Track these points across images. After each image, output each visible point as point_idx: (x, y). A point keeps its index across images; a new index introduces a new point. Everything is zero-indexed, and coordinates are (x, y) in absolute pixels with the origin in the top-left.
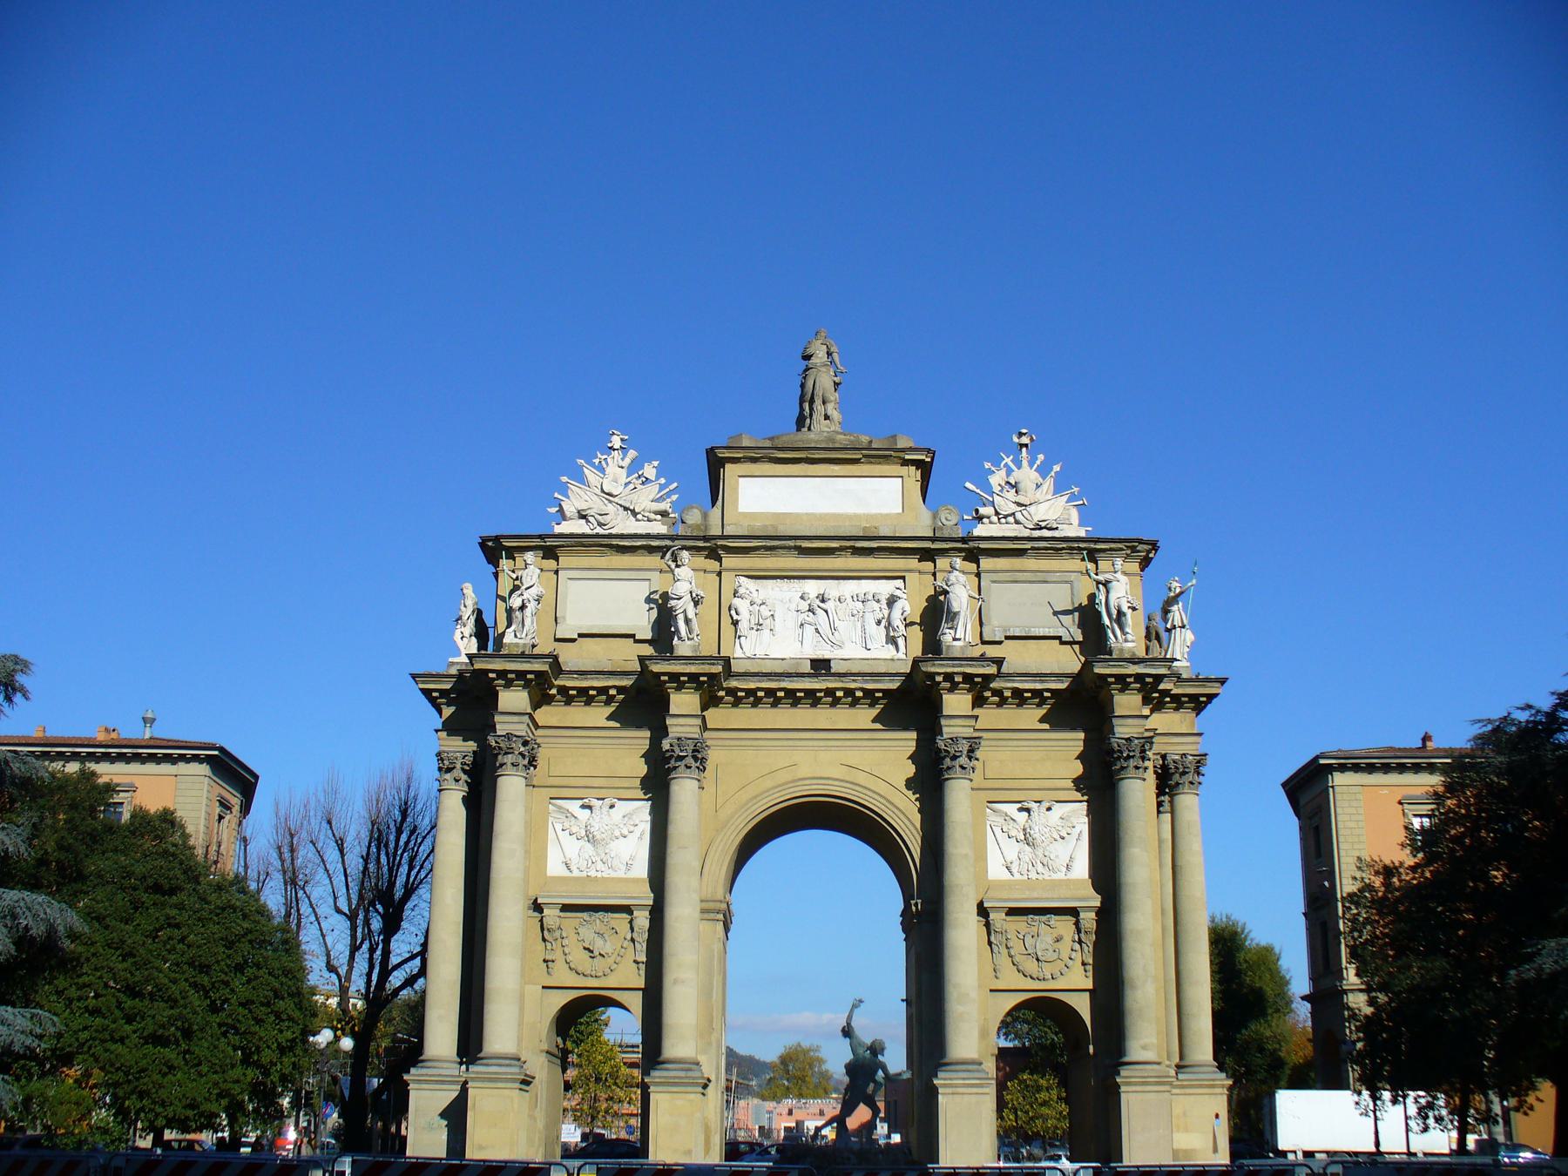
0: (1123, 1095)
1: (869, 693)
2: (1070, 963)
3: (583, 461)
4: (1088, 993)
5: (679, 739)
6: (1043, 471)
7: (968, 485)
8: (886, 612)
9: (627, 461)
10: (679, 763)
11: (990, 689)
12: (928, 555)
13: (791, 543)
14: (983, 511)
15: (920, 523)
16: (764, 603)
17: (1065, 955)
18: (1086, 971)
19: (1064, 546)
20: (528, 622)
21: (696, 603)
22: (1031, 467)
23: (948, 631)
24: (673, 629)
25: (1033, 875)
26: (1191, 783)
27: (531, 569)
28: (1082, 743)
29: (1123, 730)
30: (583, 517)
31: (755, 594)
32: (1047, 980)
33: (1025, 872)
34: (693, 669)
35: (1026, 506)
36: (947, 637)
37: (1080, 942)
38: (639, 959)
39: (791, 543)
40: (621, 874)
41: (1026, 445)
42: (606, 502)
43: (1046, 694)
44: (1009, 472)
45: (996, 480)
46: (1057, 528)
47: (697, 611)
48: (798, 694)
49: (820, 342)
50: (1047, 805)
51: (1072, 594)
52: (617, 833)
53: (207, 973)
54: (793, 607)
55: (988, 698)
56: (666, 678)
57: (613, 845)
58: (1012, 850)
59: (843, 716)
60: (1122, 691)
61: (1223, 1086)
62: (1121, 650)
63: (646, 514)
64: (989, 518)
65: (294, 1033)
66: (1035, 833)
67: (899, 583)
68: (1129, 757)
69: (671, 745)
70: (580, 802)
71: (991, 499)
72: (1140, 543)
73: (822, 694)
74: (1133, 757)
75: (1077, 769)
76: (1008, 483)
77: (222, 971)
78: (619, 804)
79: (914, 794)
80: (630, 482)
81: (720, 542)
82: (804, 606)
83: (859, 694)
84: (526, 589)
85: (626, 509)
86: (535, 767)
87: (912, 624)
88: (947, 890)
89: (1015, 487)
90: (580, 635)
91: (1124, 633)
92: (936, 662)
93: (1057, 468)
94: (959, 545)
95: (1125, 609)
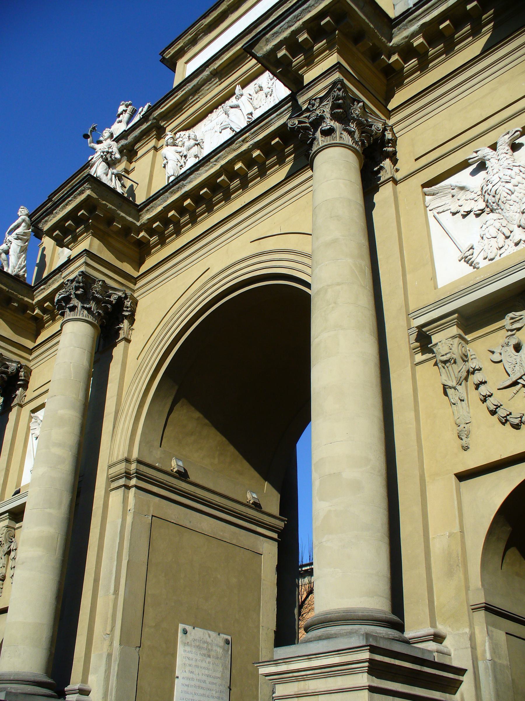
13: (206, 73)
39: (206, 73)
92: (267, 36)
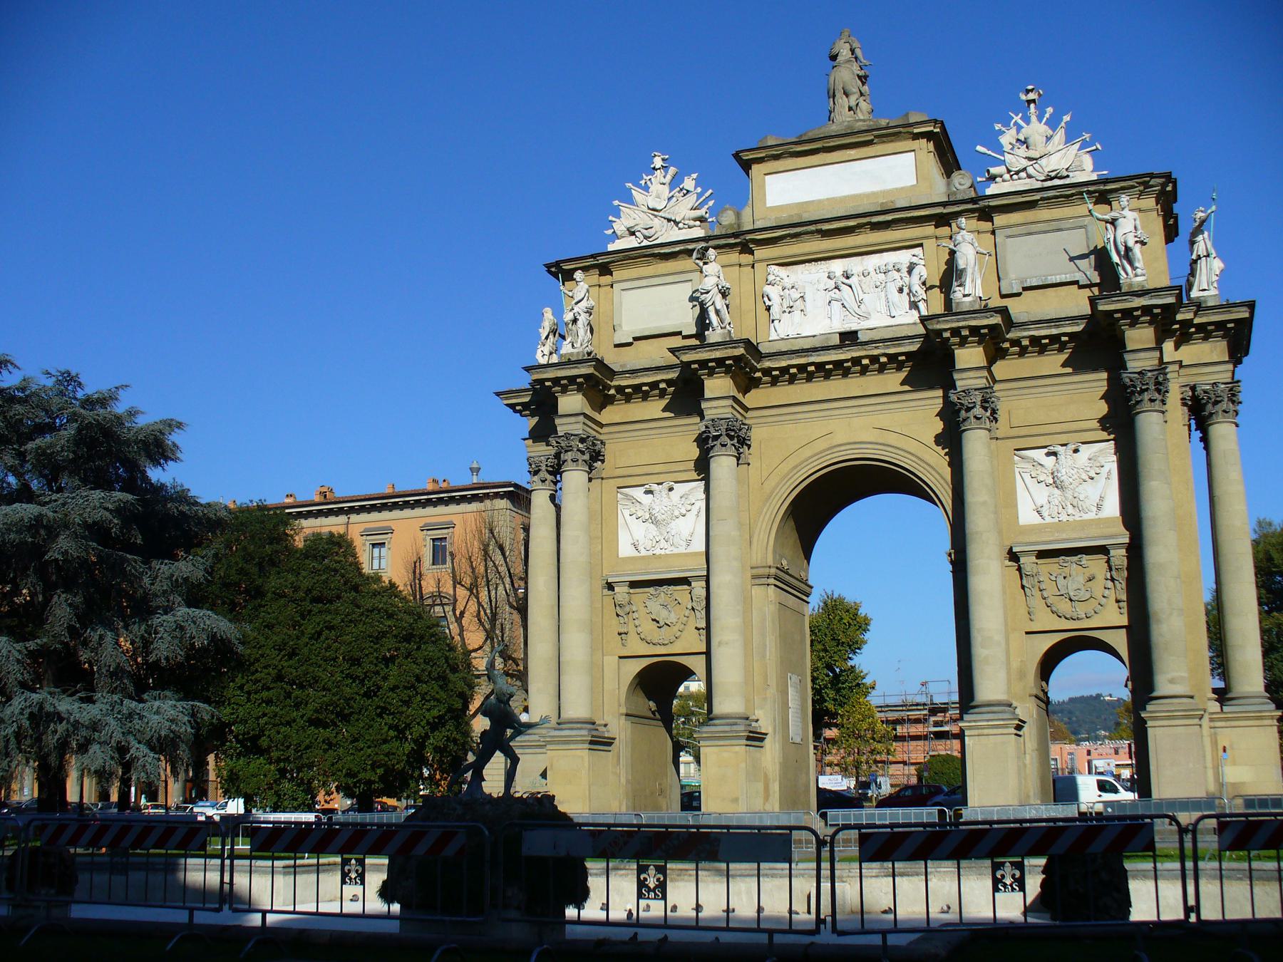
0: (1150, 731)
1: (892, 358)
2: (1103, 601)
3: (630, 185)
4: (1124, 630)
5: (713, 420)
6: (1053, 124)
7: (979, 148)
8: (907, 280)
9: (669, 177)
10: (715, 443)
11: (1007, 340)
12: (942, 220)
13: (812, 228)
14: (993, 170)
15: (936, 189)
16: (793, 287)
17: (1098, 594)
18: (1120, 608)
19: (1074, 191)
20: (581, 332)
21: (724, 294)
22: (1040, 122)
23: (957, 288)
24: (707, 322)
25: (1064, 518)
26: (1225, 411)
27: (582, 284)
28: (1105, 383)
29: (1137, 363)
30: (633, 234)
31: (786, 280)
32: (1082, 619)
33: (1055, 514)
34: (718, 354)
35: (1036, 159)
36: (958, 294)
37: (1113, 580)
38: (699, 626)
39: (812, 228)
40: (682, 550)
41: (1034, 101)
42: (652, 217)
43: (1063, 339)
44: (1019, 128)
45: (1007, 139)
46: (1068, 176)
47: (727, 302)
48: (827, 367)
49: (843, 41)
50: (1073, 447)
51: (1087, 238)
52: (676, 513)
53: (359, 665)
54: (822, 287)
55: (1008, 349)
56: (696, 366)
57: (673, 524)
58: (1043, 495)
59: (873, 383)
60: (1132, 325)
61: (1272, 718)
62: (1131, 285)
63: (686, 222)
64: (1001, 176)
65: (440, 711)
66: (1063, 475)
67: (918, 251)
68: (1142, 391)
69: (707, 427)
70: (642, 489)
71: (1003, 158)
72: (1152, 178)
73: (849, 364)
74: (1147, 390)
75: (1103, 408)
76: (1018, 140)
77: (371, 662)
78: (676, 486)
79: (943, 449)
80: (673, 196)
81: (749, 237)
82: (831, 284)
83: (883, 359)
84: (577, 303)
85: (669, 220)
86: (603, 461)
87: (932, 287)
88: (969, 537)
89: (1025, 142)
90: (636, 339)
91: (1134, 268)
93: (1067, 118)
94: (970, 206)
95: (1131, 243)
